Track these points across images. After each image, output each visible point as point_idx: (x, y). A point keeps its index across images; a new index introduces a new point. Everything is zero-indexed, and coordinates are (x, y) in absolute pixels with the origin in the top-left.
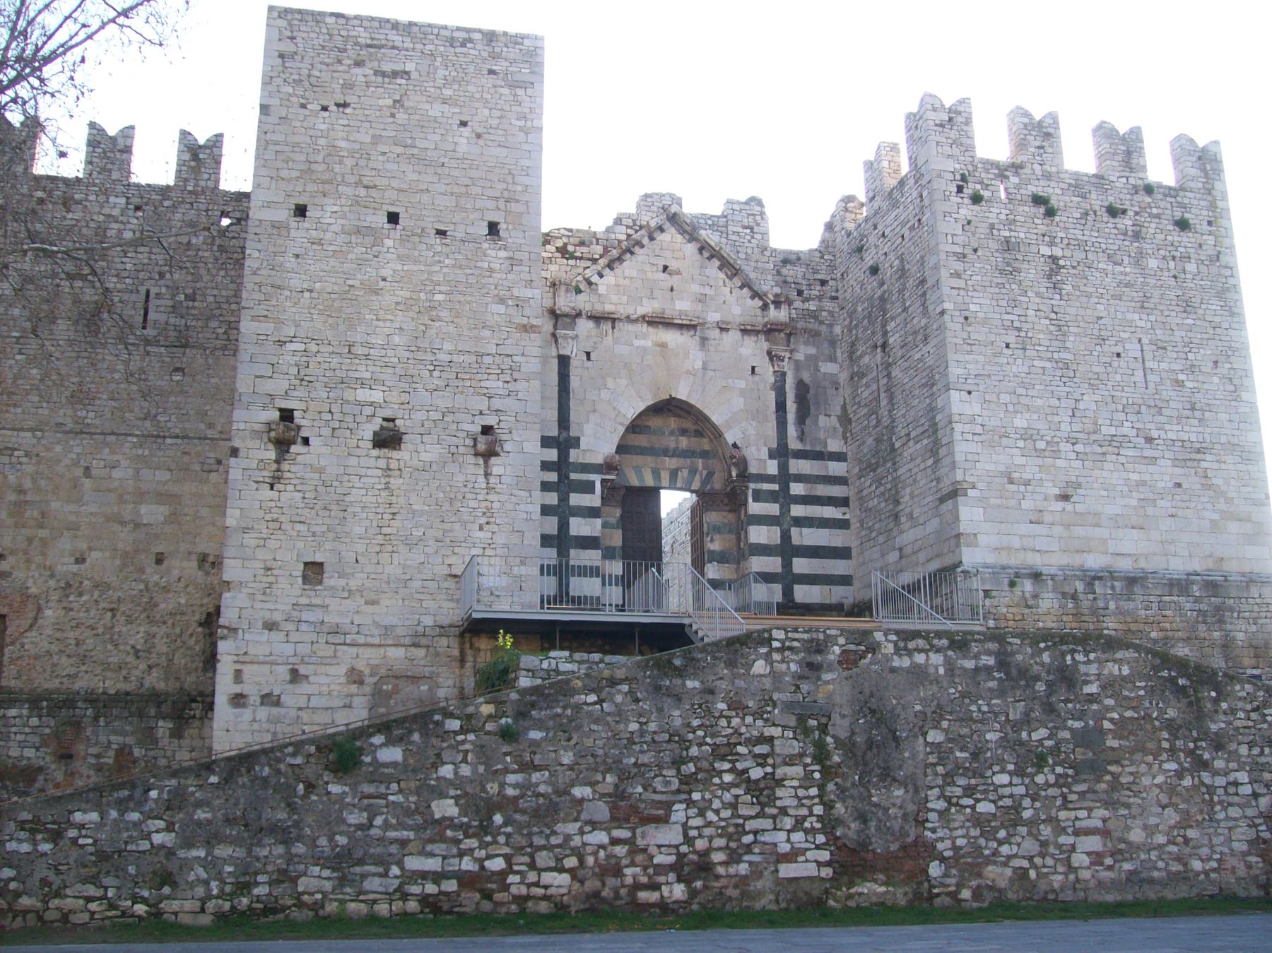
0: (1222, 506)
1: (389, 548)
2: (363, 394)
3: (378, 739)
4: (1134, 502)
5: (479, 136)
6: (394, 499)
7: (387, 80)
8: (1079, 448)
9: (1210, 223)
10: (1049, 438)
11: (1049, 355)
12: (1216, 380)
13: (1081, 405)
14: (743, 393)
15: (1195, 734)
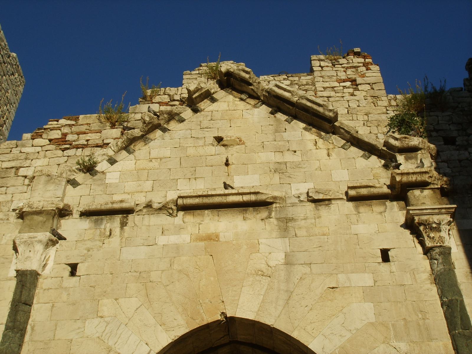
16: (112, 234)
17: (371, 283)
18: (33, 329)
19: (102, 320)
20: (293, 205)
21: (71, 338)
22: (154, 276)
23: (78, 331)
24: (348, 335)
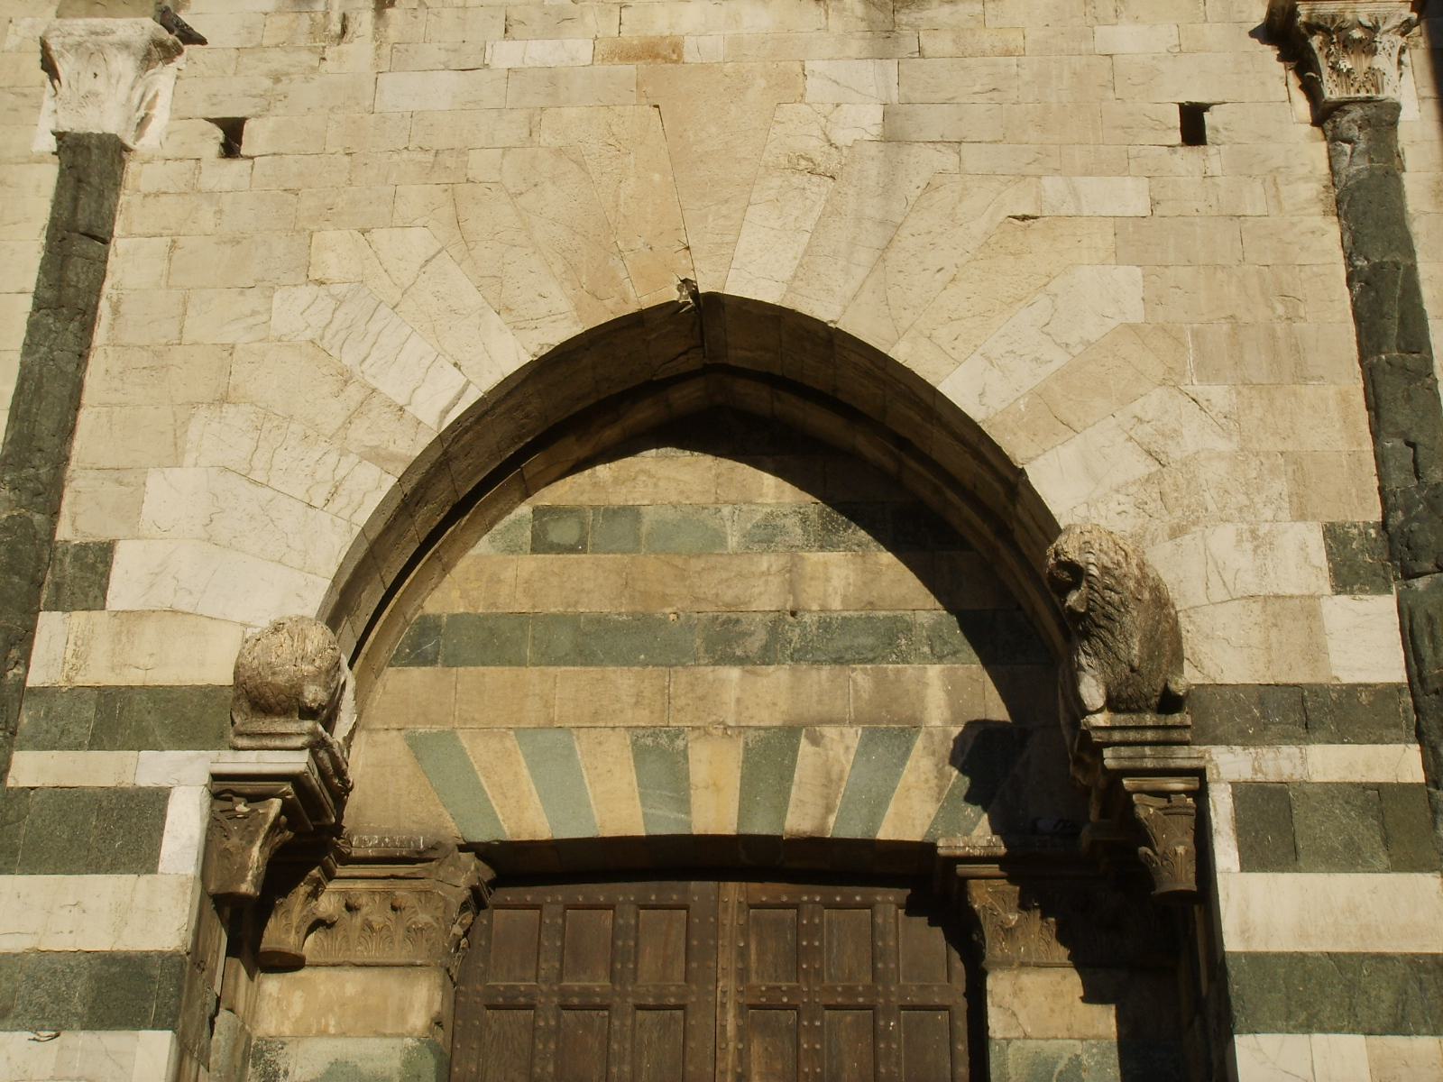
16: (350, 29)
18: (116, 310)
19: (322, 291)
21: (230, 341)
22: (479, 163)
23: (251, 321)
24: (1059, 359)
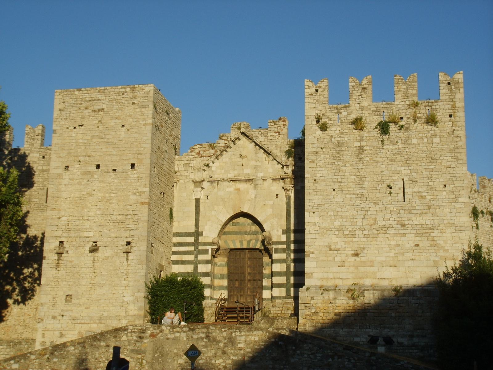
0: (441, 253)
1: (93, 288)
2: (87, 234)
3: (12, 362)
4: (392, 255)
5: (128, 130)
6: (96, 271)
7: (96, 113)
8: (365, 232)
9: (450, 116)
10: (351, 229)
11: (355, 192)
12: (444, 193)
13: (369, 213)
14: (272, 207)
15: (284, 362)
17: (272, 204)
20: (258, 180)
